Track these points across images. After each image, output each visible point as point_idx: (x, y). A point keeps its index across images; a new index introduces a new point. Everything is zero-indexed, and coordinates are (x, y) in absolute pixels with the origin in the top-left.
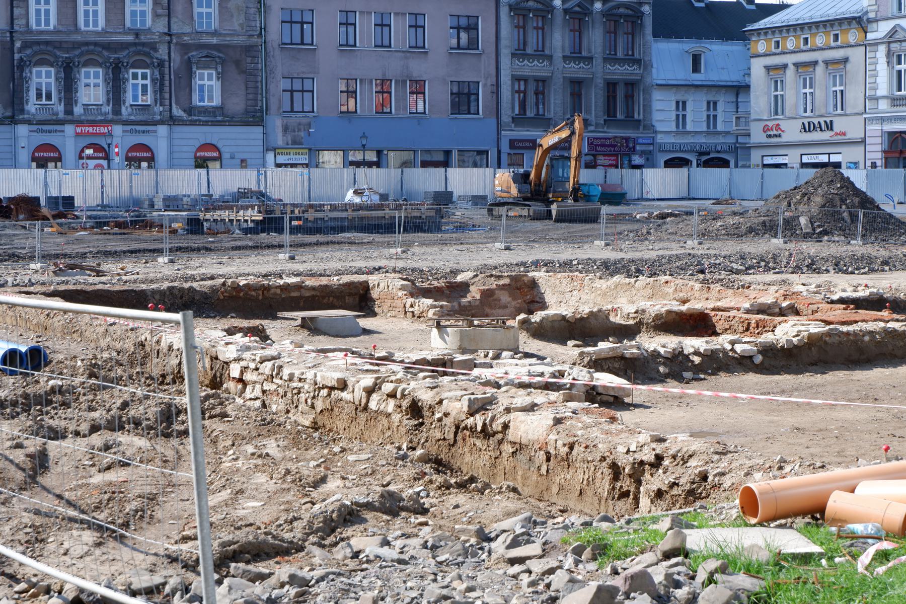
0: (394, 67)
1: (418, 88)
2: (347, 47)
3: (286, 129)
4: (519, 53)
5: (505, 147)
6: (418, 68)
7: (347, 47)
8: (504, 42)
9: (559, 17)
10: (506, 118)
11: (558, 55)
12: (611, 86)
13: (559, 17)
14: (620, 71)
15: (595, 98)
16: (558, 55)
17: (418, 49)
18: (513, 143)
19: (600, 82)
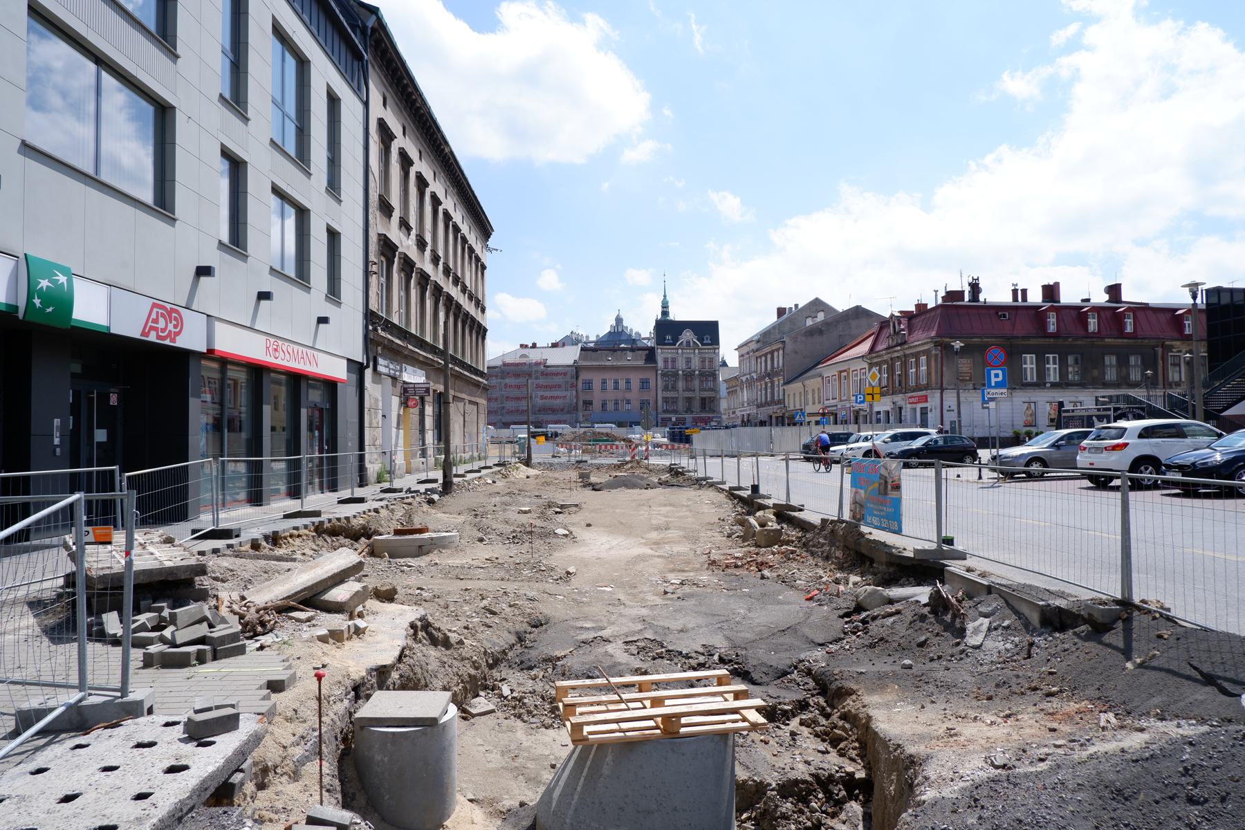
0: (619, 395)
1: (628, 402)
2: (604, 389)
3: (583, 416)
4: (666, 388)
5: (659, 421)
6: (628, 396)
7: (604, 389)
8: (659, 386)
9: (681, 377)
10: (660, 410)
11: (681, 389)
12: (703, 400)
13: (681, 377)
14: (706, 394)
15: (696, 405)
16: (681, 389)
17: (628, 389)
18: (662, 419)
19: (698, 398)
